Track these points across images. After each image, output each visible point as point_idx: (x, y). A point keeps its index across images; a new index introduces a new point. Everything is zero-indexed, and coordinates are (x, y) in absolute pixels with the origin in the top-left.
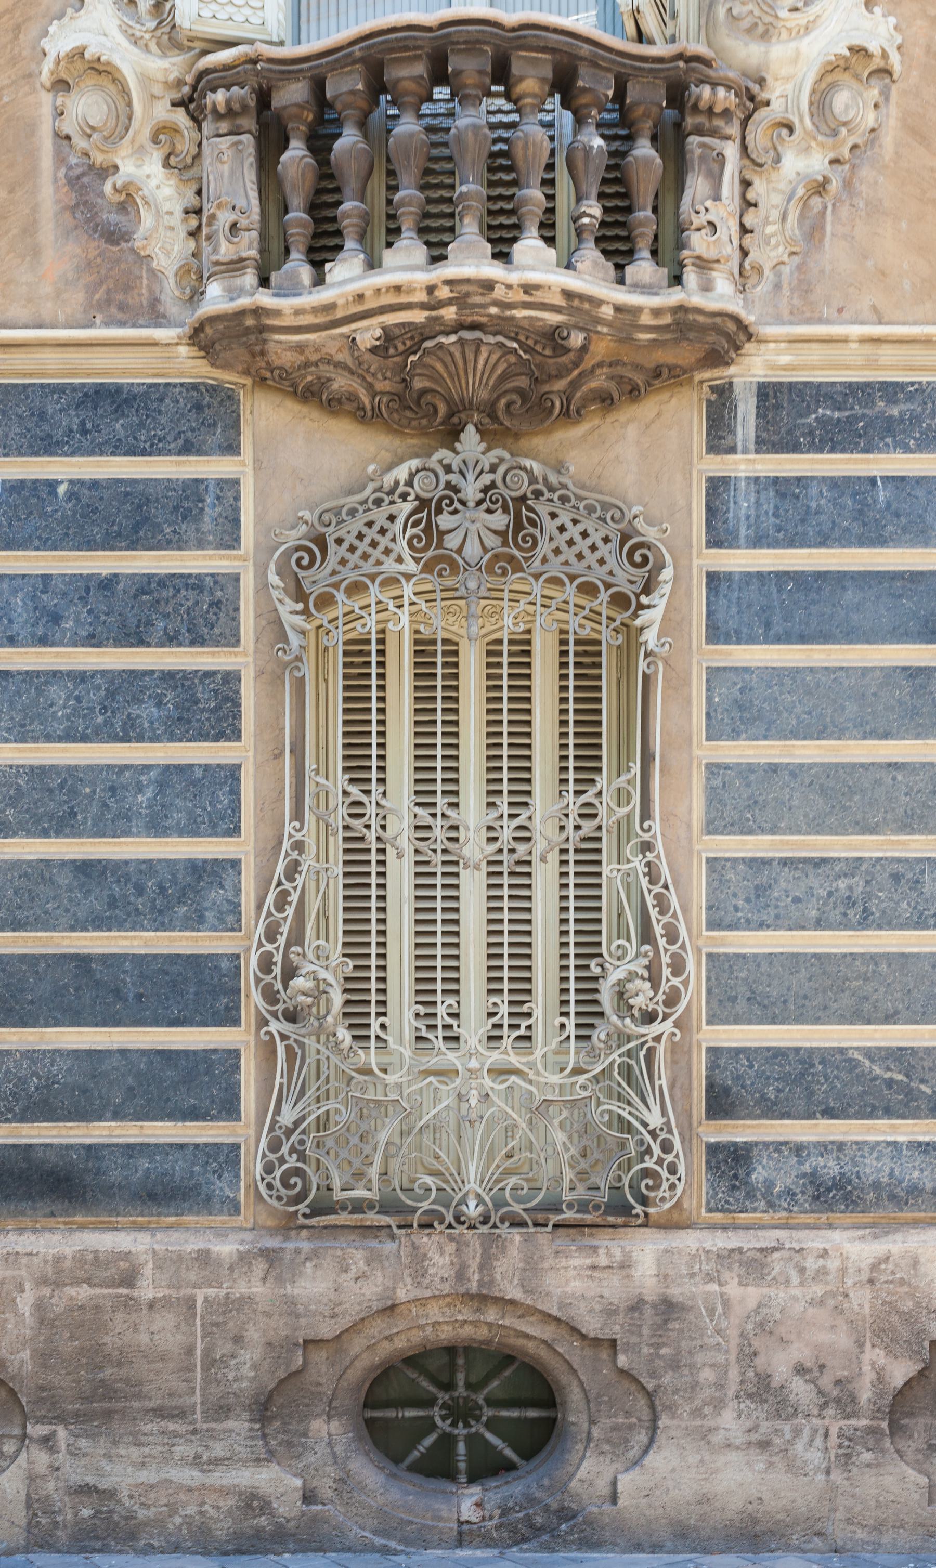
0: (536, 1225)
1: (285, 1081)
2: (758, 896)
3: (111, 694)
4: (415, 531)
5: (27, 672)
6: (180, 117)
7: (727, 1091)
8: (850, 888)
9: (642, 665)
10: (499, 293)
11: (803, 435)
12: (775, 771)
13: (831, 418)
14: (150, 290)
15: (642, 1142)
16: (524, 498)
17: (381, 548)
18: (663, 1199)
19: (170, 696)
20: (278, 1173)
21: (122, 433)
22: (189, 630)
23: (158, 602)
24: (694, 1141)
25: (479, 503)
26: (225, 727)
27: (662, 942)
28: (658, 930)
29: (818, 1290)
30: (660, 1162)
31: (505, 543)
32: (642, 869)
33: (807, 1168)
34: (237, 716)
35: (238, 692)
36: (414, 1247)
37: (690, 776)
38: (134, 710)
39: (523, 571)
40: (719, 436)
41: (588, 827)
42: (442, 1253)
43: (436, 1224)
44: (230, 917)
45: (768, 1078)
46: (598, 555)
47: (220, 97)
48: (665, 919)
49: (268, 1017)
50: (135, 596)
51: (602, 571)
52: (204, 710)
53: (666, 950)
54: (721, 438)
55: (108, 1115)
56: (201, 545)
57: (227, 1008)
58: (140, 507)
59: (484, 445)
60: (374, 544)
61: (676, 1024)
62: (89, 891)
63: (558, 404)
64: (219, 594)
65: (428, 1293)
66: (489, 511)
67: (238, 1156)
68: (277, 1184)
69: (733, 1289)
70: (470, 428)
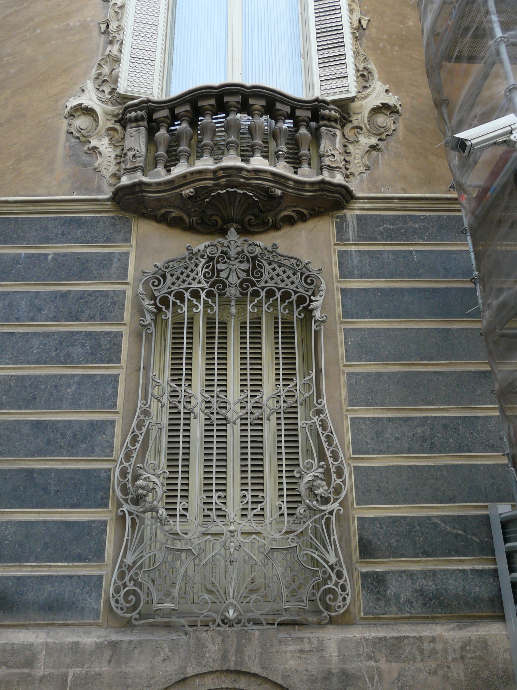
0: (268, 624)
1: (129, 538)
2: (378, 437)
3: (61, 343)
4: (207, 270)
5: (23, 333)
6: (118, 126)
7: (370, 542)
8: (423, 432)
9: (313, 327)
10: (244, 174)
11: (379, 234)
12: (380, 376)
13: (390, 229)
14: (98, 182)
15: (325, 572)
16: (256, 256)
17: (191, 277)
18: (339, 607)
20: (122, 593)
21: (80, 235)
22: (100, 314)
23: (87, 302)
24: (354, 572)
27: (331, 460)
28: (328, 454)
29: (432, 664)
30: (336, 584)
31: (248, 275)
32: (318, 423)
33: (417, 586)
34: (119, 352)
35: (121, 341)
36: (198, 640)
37: (340, 379)
38: (71, 350)
39: (256, 286)
40: (341, 235)
41: (290, 400)
42: (214, 643)
43: (210, 624)
44: (108, 449)
45: (391, 534)
46: (291, 280)
47: (133, 114)
49: (123, 502)
50: (77, 300)
51: (293, 287)
52: (104, 349)
53: (333, 465)
54: (342, 235)
55: (32, 558)
56: (109, 278)
58: (84, 263)
60: (188, 276)
61: (341, 504)
62: (38, 436)
63: (271, 220)
64: (116, 299)
65: (205, 670)
66: (241, 262)
67: (101, 583)
68: (121, 600)
69: (383, 665)
70: (232, 229)
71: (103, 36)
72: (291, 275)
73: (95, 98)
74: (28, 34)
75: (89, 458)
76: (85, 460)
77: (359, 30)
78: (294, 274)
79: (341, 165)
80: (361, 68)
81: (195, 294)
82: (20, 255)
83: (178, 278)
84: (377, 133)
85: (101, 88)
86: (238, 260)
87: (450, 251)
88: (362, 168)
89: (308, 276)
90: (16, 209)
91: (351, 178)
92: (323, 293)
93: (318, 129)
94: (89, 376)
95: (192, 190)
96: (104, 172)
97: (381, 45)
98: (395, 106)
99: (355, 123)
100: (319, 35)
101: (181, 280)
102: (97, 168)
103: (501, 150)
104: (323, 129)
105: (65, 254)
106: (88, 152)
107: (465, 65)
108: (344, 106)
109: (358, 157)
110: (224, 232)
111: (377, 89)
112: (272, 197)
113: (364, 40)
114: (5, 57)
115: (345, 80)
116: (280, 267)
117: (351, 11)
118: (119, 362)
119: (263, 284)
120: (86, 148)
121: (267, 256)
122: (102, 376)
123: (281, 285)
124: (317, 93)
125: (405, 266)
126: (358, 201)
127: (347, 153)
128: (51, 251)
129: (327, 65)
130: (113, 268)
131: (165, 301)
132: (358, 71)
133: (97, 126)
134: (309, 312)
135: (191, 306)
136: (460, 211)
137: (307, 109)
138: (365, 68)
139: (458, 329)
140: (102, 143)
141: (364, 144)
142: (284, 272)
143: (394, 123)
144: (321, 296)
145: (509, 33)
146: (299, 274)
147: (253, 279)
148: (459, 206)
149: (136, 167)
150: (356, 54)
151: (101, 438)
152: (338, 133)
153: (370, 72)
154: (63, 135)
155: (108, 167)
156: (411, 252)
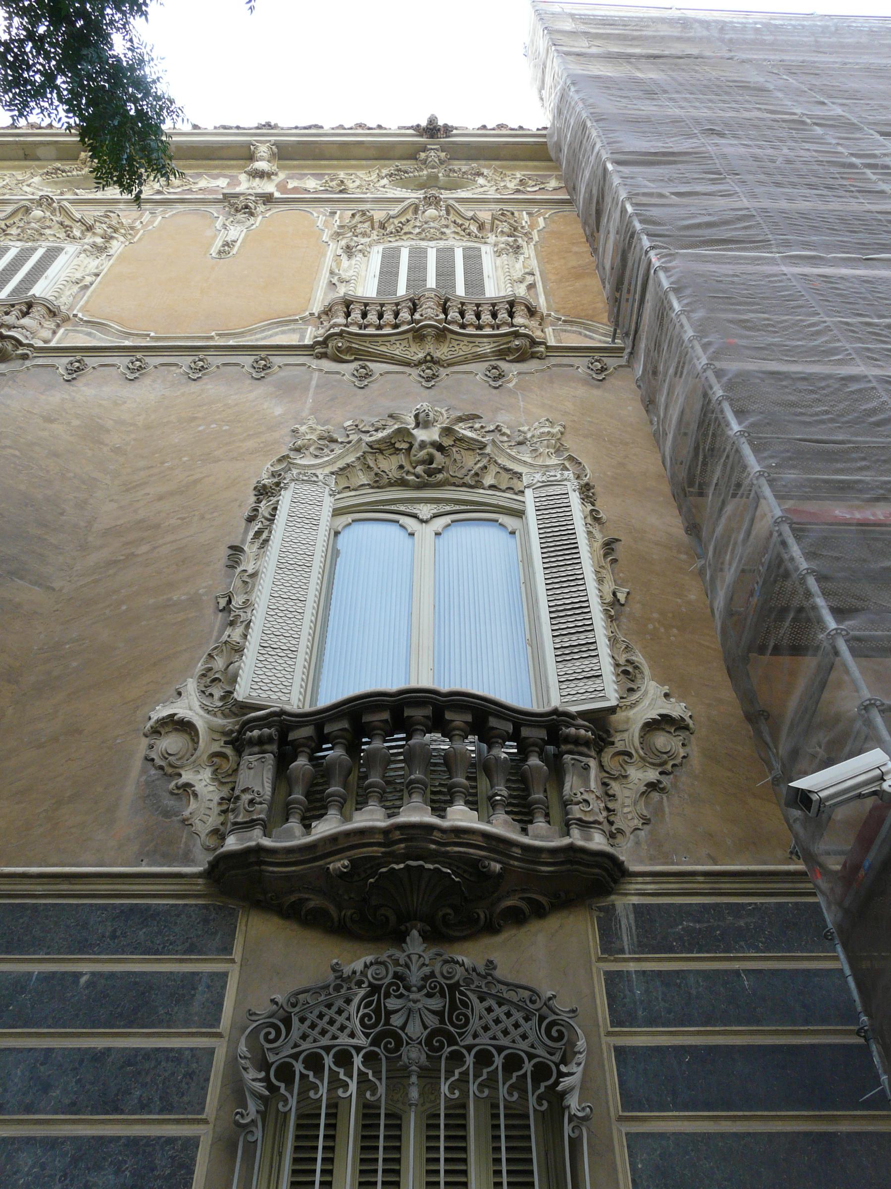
4: (366, 1011)
6: (229, 751)
9: (567, 1129)
10: (436, 835)
14: (186, 843)
16: (457, 984)
17: (337, 1025)
22: (161, 1099)
31: (442, 1021)
35: (193, 1159)
39: (457, 1044)
40: (609, 944)
46: (520, 1030)
47: (256, 733)
50: (122, 1067)
51: (524, 1045)
52: (158, 1177)
54: (611, 943)
56: (187, 1023)
58: (143, 993)
59: (425, 945)
60: (332, 1022)
63: (482, 916)
64: (194, 1066)
66: (429, 995)
70: (415, 933)
71: (220, 614)
73: (196, 705)
74: (107, 611)
77: (614, 608)
78: (527, 1019)
79: (601, 818)
80: (622, 661)
81: (344, 1058)
82: (30, 974)
83: (313, 1026)
84: (658, 761)
85: (210, 690)
86: (425, 991)
87: (808, 970)
88: (636, 821)
90: (39, 889)
91: (619, 839)
92: (581, 1057)
93: (558, 756)
95: (346, 862)
96: (199, 826)
97: (650, 626)
98: (682, 719)
99: (619, 746)
100: (553, 615)
101: (318, 1029)
102: (187, 820)
103: (869, 802)
104: (567, 757)
105: (112, 975)
106: (176, 791)
107: (785, 660)
108: (600, 722)
109: (628, 802)
110: (399, 938)
111: (651, 691)
112: (485, 876)
113: (624, 620)
114: (67, 643)
115: (598, 681)
116: (500, 1005)
117: (600, 581)
119: (469, 1041)
120: (172, 785)
121: (476, 983)
123: (504, 1041)
124: (555, 702)
125: (728, 1000)
126: (633, 880)
127: (609, 796)
128: (86, 967)
129: (568, 658)
130: (196, 1004)
131: (285, 1073)
132: (617, 665)
133: (195, 750)
134: (556, 1100)
135: (336, 1083)
136: (814, 894)
137: (540, 726)
138: (628, 661)
139: (849, 1135)
140: (200, 777)
141: (636, 781)
142: (508, 1015)
143: (683, 745)
144: (579, 1064)
145: (847, 623)
146: (535, 1019)
147: (452, 1029)
148: (811, 885)
149: (253, 821)
150: (613, 641)
152: (593, 763)
153: (636, 668)
154: (138, 763)
155: (205, 818)
156: (737, 973)
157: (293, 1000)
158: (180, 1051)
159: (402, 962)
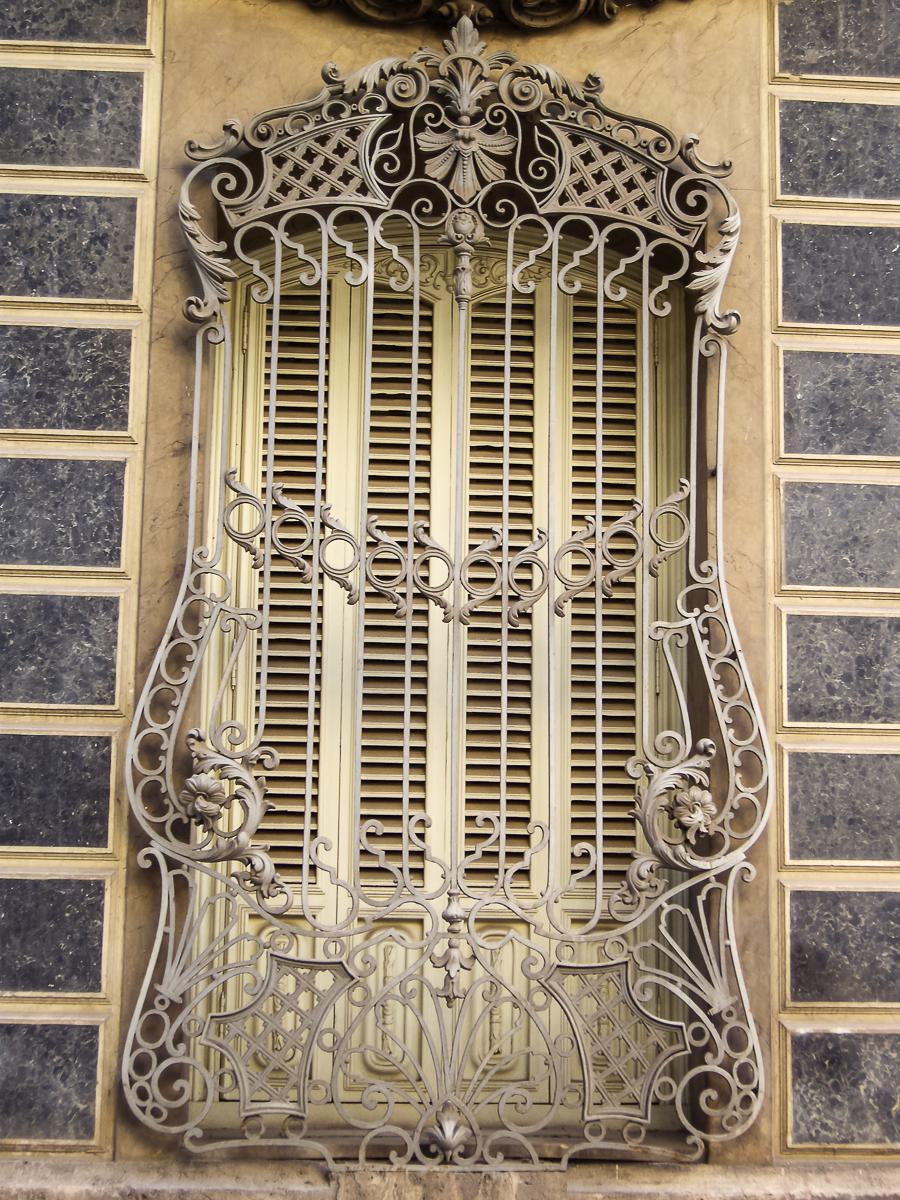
0: (543, 1159)
1: (171, 930)
2: (861, 674)
4: (386, 151)
7: (821, 957)
9: (698, 345)
12: (881, 498)
15: (698, 1034)
18: (733, 1121)
19: (28, 362)
20: (156, 1072)
22: (60, 275)
23: (18, 233)
24: (775, 1034)
25: (475, 119)
26: (103, 406)
27: (728, 734)
28: (723, 717)
30: (728, 1065)
31: (510, 174)
34: (123, 394)
35: (125, 361)
37: (763, 500)
39: (533, 211)
43: (393, 1155)
44: (97, 683)
45: (881, 939)
48: (733, 702)
49: (150, 832)
52: (75, 384)
53: (735, 747)
56: (84, 156)
57: (88, 819)
59: (483, 44)
60: (328, 167)
61: (750, 856)
64: (106, 225)
66: (489, 130)
67: (94, 1046)
68: (154, 1090)
70: (466, 22)
72: (639, 179)
75: (44, 706)
76: (32, 711)
83: (297, 172)
86: (482, 124)
89: (693, 185)
92: (733, 242)
94: (39, 466)
101: (306, 178)
110: (440, 26)
116: (605, 150)
118: (124, 425)
119: (552, 206)
121: (568, 113)
122: (75, 465)
123: (608, 210)
130: (94, 125)
134: (688, 301)
142: (618, 167)
144: (726, 251)
146: (662, 177)
151: (79, 649)
157: (263, 129)
158: (78, 201)
159: (443, 71)
